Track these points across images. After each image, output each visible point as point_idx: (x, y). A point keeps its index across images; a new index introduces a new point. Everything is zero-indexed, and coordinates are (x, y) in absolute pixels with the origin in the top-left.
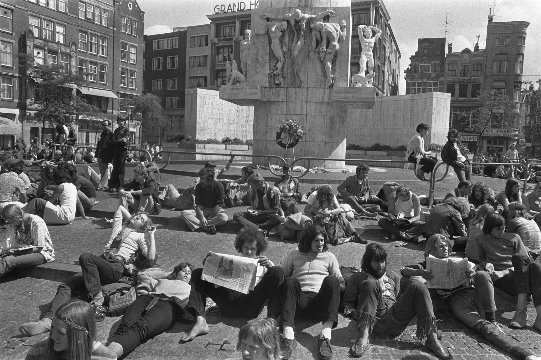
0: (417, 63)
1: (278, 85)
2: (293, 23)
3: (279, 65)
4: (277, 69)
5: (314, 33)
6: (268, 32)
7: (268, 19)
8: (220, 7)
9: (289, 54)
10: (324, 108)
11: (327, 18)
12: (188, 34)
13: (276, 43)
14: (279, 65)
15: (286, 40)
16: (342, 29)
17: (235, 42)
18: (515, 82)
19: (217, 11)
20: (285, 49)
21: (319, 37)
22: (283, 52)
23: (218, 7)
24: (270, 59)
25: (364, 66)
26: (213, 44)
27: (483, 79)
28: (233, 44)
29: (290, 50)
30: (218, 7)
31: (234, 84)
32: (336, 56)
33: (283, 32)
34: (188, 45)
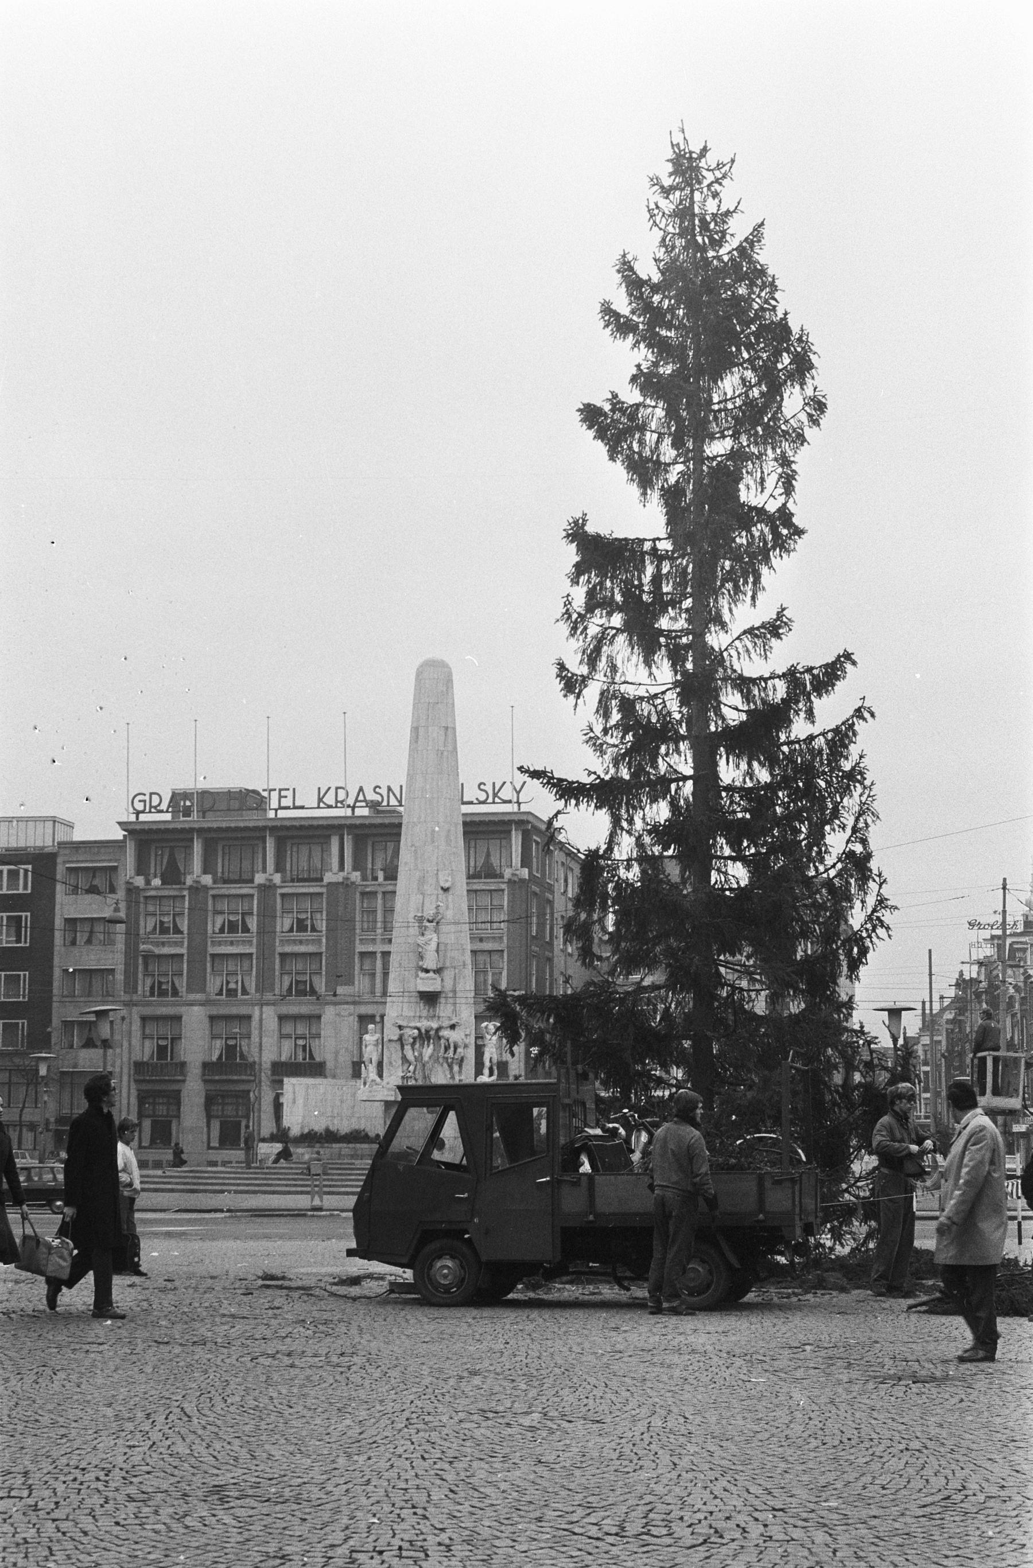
7: (400, 1027)
8: (147, 798)
11: (453, 1027)
12: (59, 860)
13: (408, 1048)
14: (412, 1068)
15: (417, 1046)
17: (190, 888)
19: (140, 806)
20: (416, 1054)
23: (141, 797)
25: (487, 1064)
26: (132, 890)
28: (186, 893)
29: (421, 1054)
30: (141, 797)
33: (415, 1039)
34: (59, 887)
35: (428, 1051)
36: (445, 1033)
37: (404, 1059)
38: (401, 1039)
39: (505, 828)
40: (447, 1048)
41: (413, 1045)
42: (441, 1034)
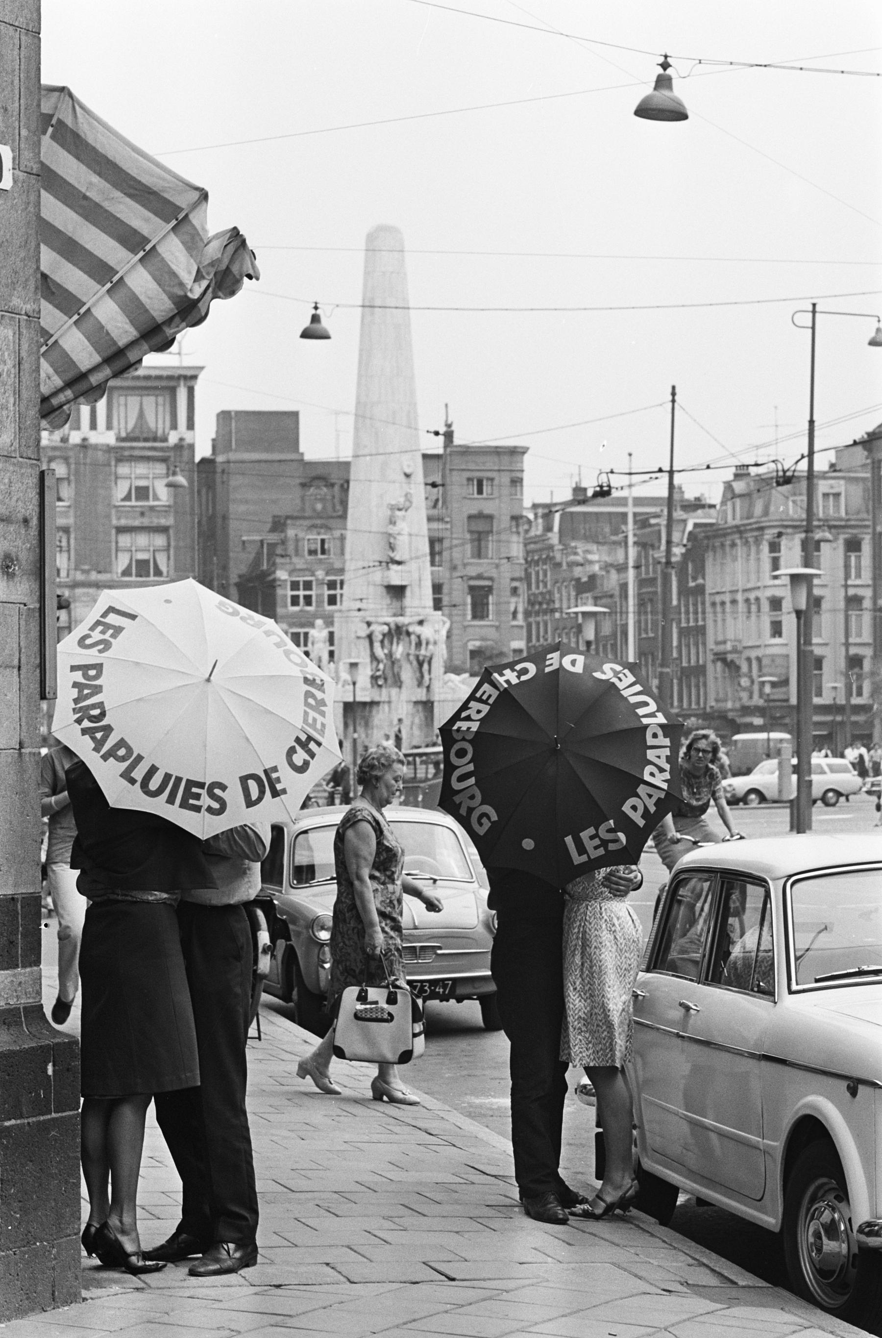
0: (301, 535)
1: (380, 686)
2: (393, 626)
3: (381, 666)
4: (379, 670)
5: (413, 637)
6: (370, 637)
7: (369, 624)
9: (390, 655)
10: (420, 708)
11: (421, 623)
13: (377, 645)
14: (381, 666)
15: (386, 642)
16: (436, 631)
18: (513, 579)
21: (417, 640)
22: (385, 654)
24: (372, 662)
27: (447, 575)
31: (343, 686)
32: (431, 659)
33: (384, 635)
35: (399, 650)
36: (415, 629)
37: (374, 657)
38: (370, 637)
39: (172, 384)
40: (419, 644)
41: (382, 642)
42: (411, 629)
